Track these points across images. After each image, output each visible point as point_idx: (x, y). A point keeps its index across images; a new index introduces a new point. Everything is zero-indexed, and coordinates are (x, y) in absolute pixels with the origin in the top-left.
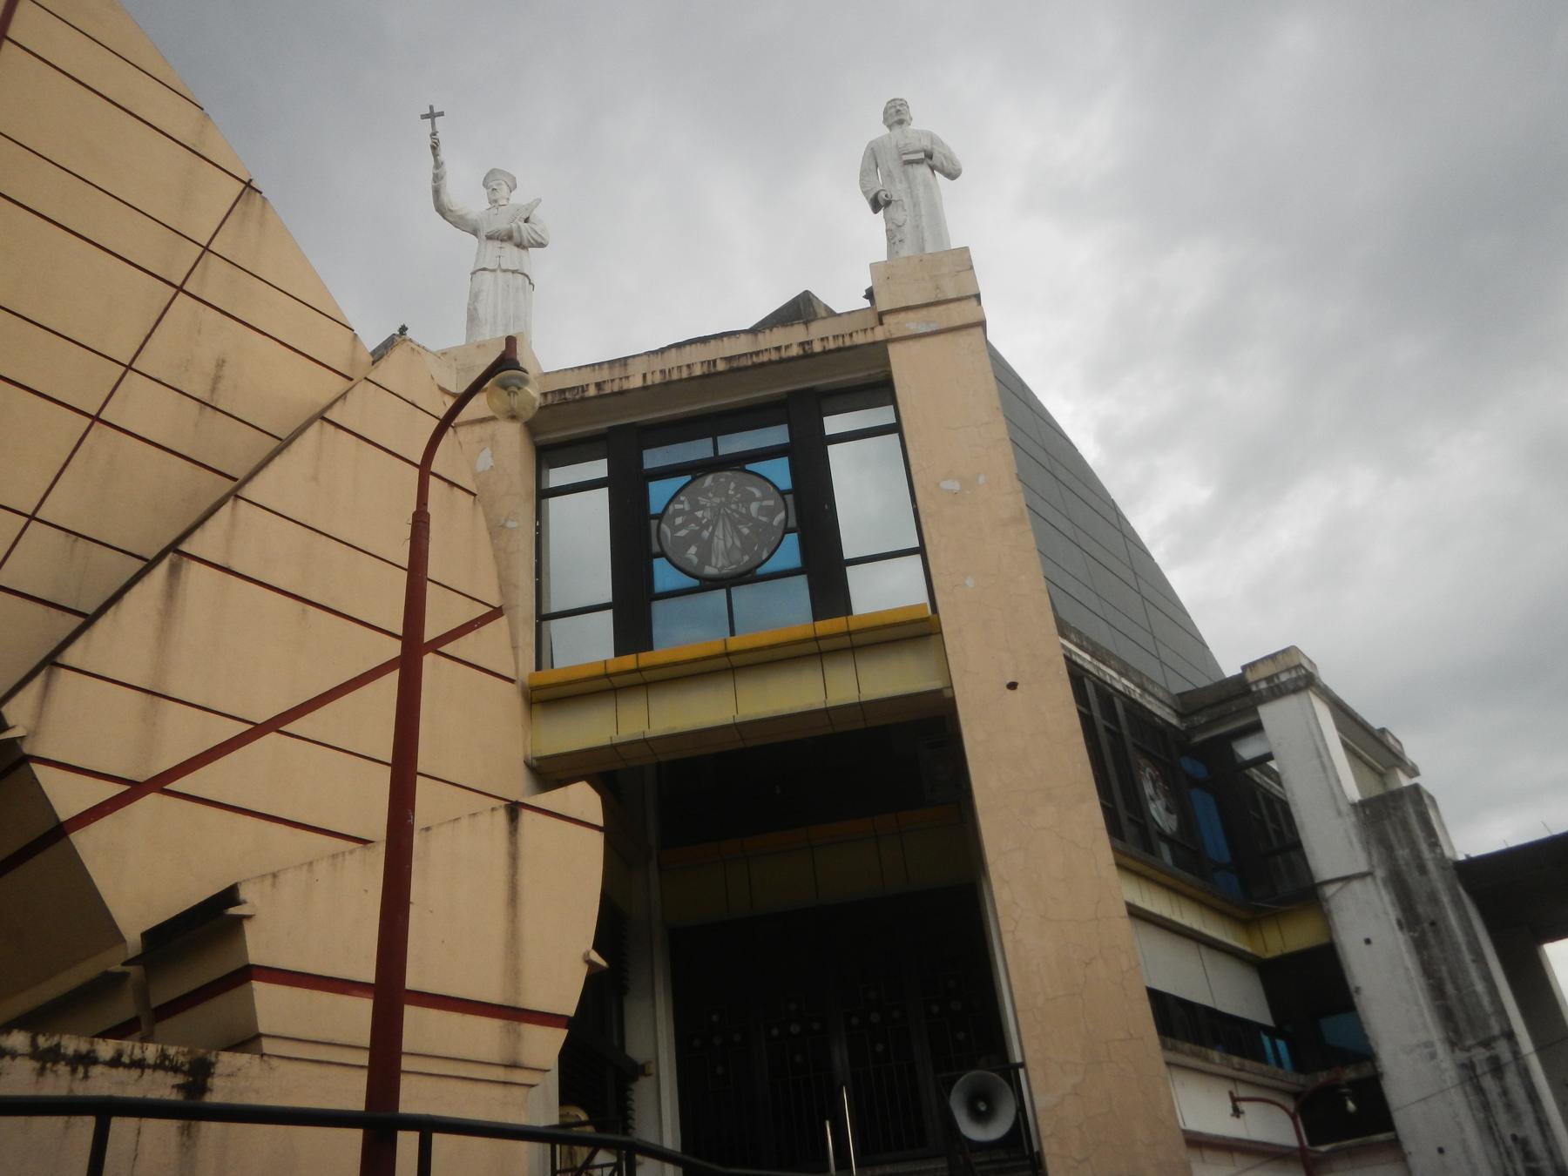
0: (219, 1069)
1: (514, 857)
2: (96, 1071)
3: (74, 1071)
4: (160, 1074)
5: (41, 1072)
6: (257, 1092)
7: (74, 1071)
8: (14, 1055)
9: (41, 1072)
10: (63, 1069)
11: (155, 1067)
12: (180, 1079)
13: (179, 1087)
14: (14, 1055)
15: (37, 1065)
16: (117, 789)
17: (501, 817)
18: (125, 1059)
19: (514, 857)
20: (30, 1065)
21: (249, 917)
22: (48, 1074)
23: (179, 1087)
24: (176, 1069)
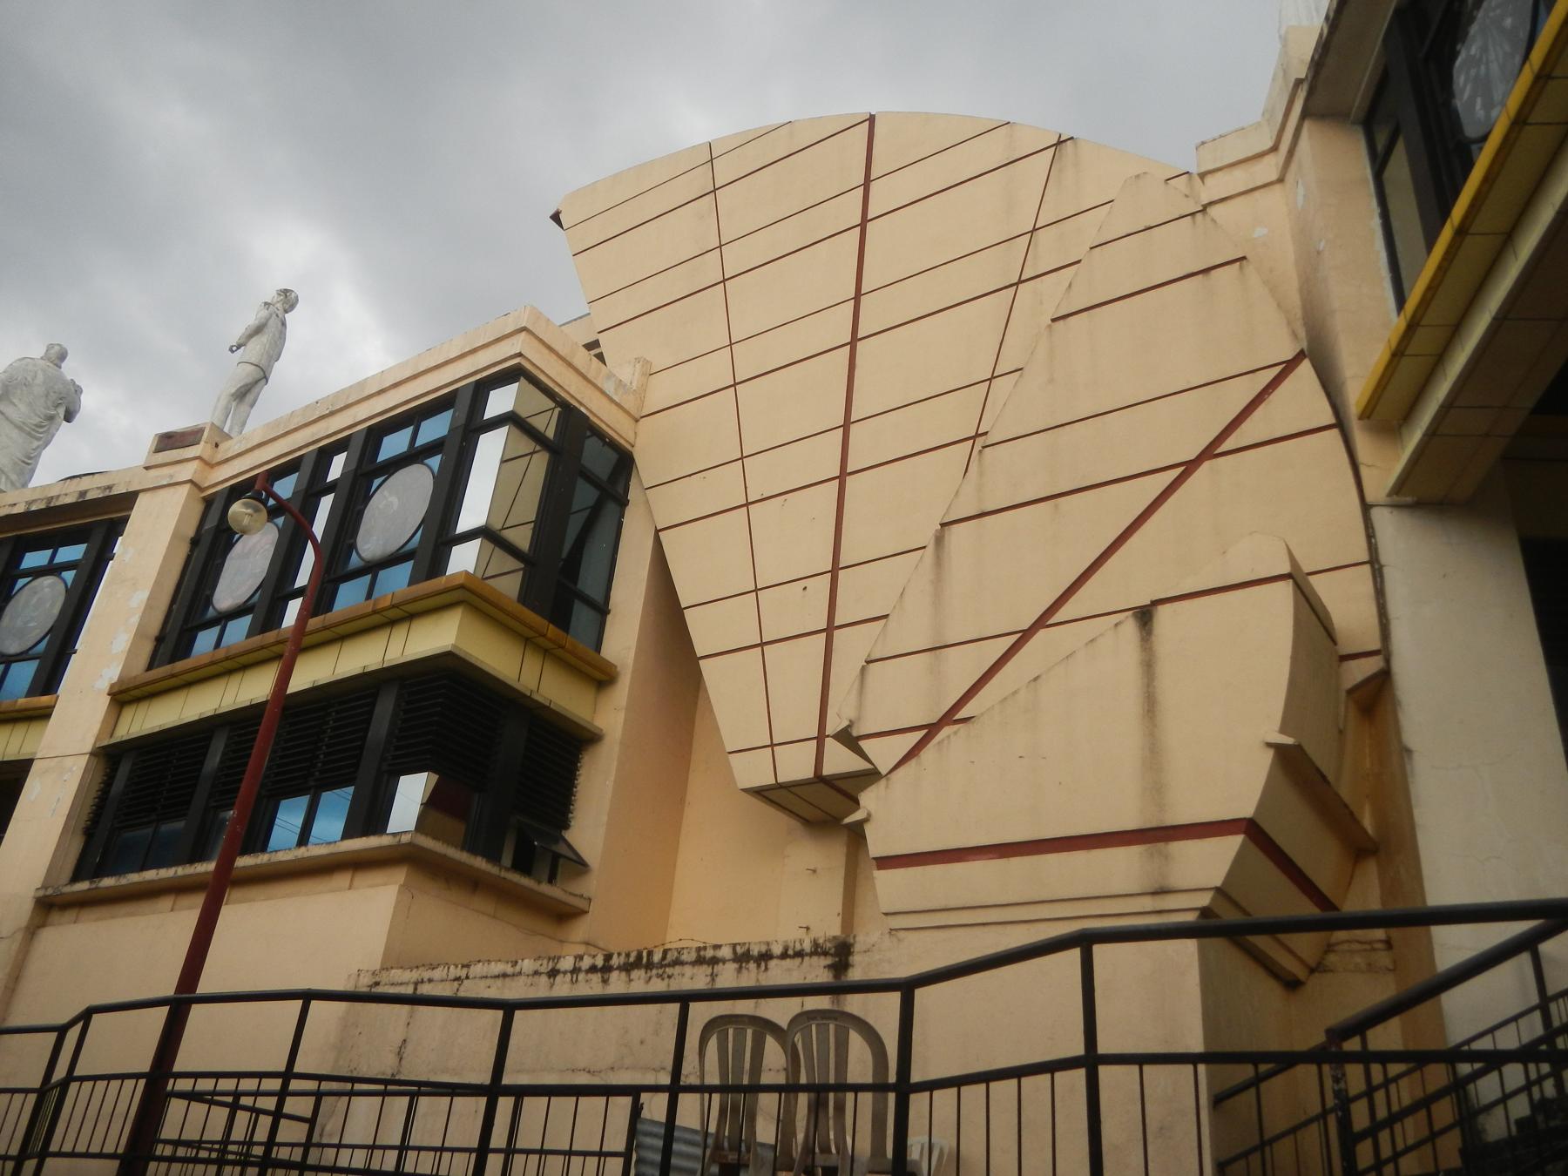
0: (857, 948)
1: (1148, 666)
2: (772, 963)
3: (759, 966)
4: (815, 958)
5: (739, 970)
6: (890, 962)
7: (759, 966)
8: (724, 961)
9: (739, 970)
10: (752, 965)
11: (811, 954)
12: (829, 961)
13: (829, 967)
14: (724, 961)
15: (736, 966)
16: (919, 735)
17: (1130, 627)
18: (790, 952)
19: (1148, 666)
20: (732, 966)
21: (866, 820)
22: (744, 971)
23: (829, 967)
24: (825, 954)
